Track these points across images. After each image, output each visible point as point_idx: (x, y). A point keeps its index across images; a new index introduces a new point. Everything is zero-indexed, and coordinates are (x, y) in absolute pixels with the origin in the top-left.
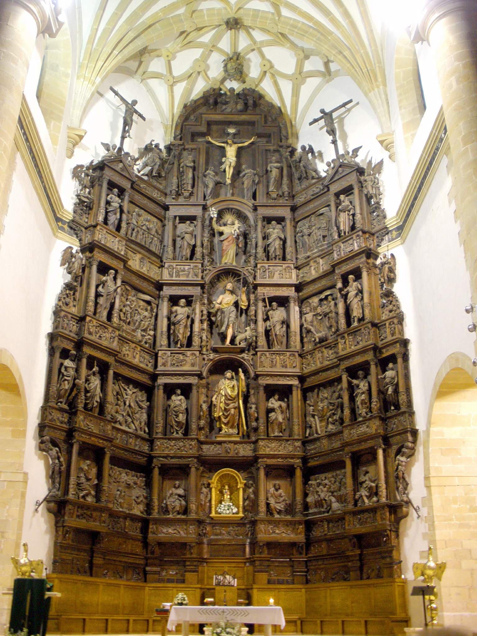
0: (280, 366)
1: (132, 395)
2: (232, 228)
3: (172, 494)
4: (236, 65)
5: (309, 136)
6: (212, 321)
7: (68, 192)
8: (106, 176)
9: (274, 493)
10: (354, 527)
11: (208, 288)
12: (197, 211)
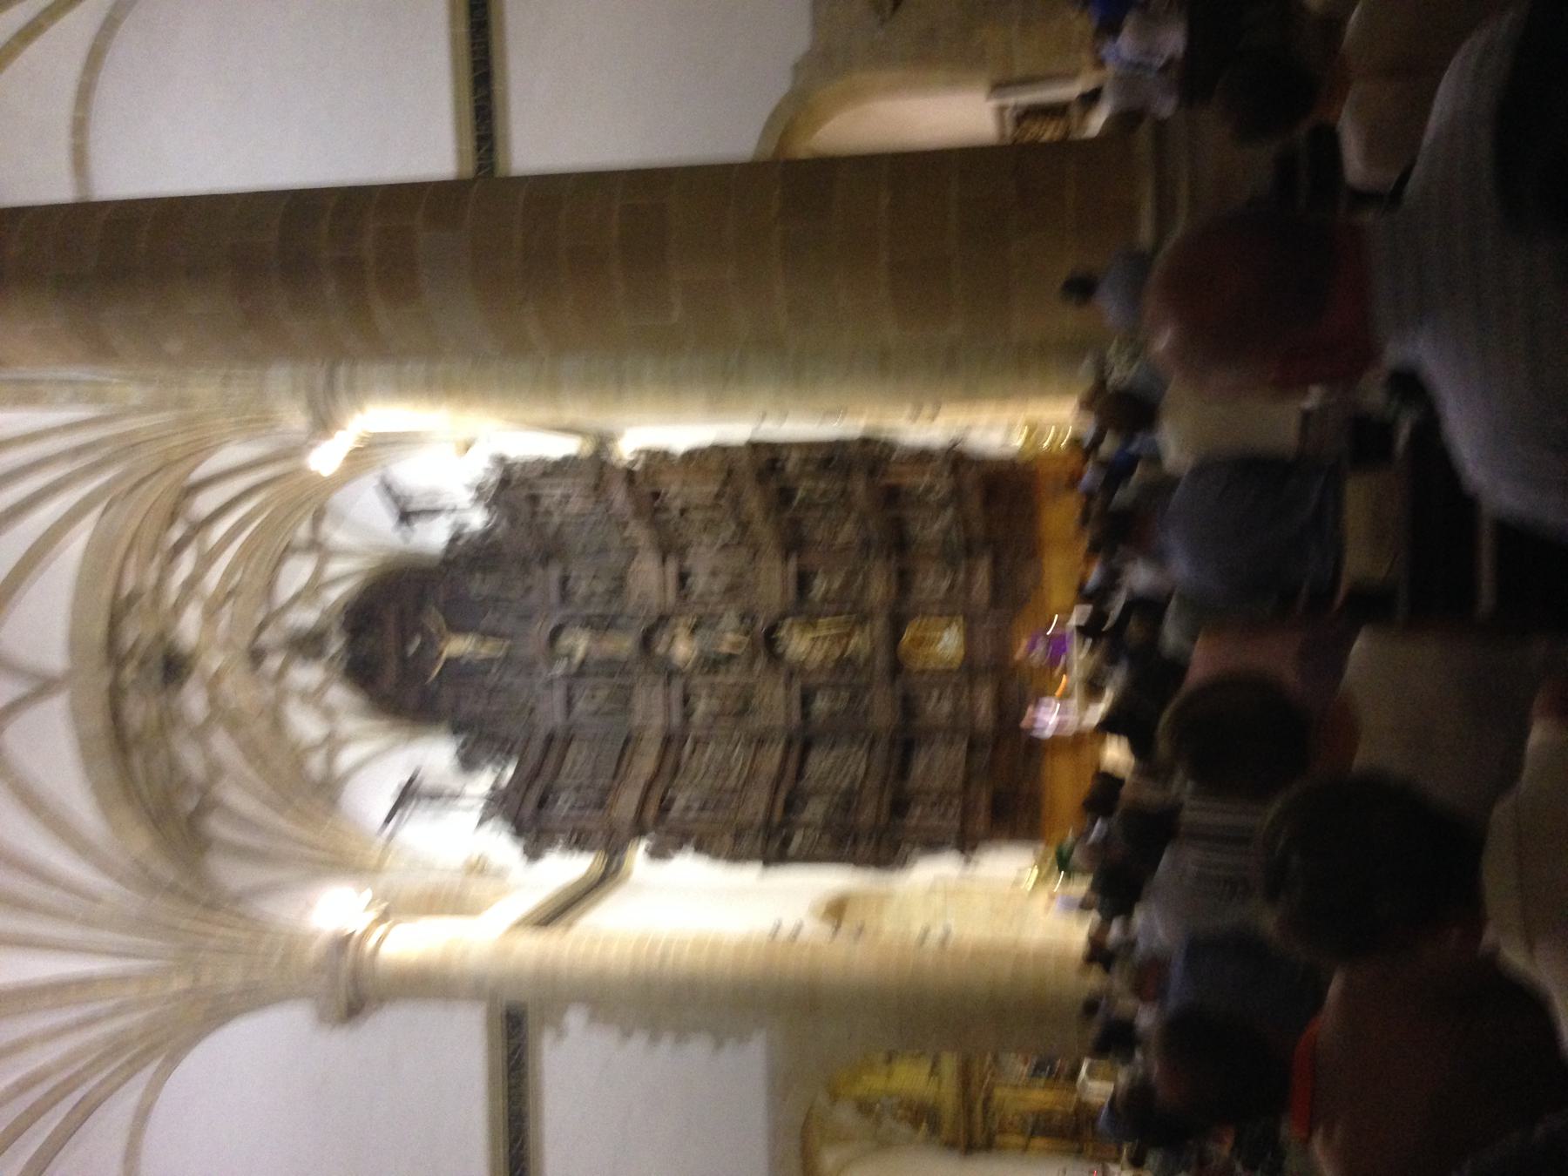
0: (772, 581)
1: (820, 763)
2: (579, 643)
3: (938, 707)
4: (307, 645)
5: (433, 537)
6: (712, 663)
7: (566, 867)
8: (531, 817)
9: (932, 583)
10: (974, 504)
11: (670, 672)
12: (559, 694)
